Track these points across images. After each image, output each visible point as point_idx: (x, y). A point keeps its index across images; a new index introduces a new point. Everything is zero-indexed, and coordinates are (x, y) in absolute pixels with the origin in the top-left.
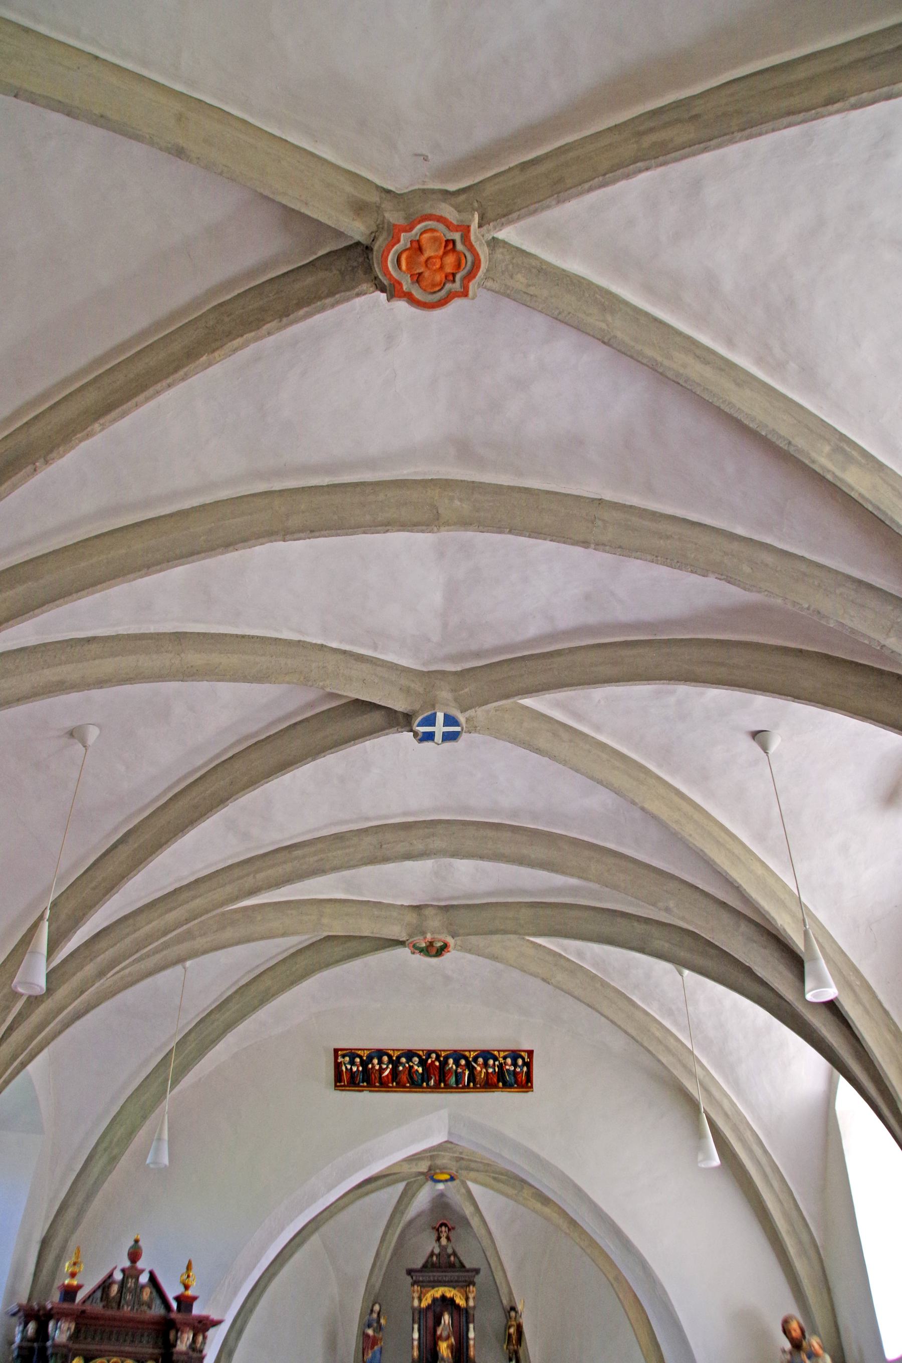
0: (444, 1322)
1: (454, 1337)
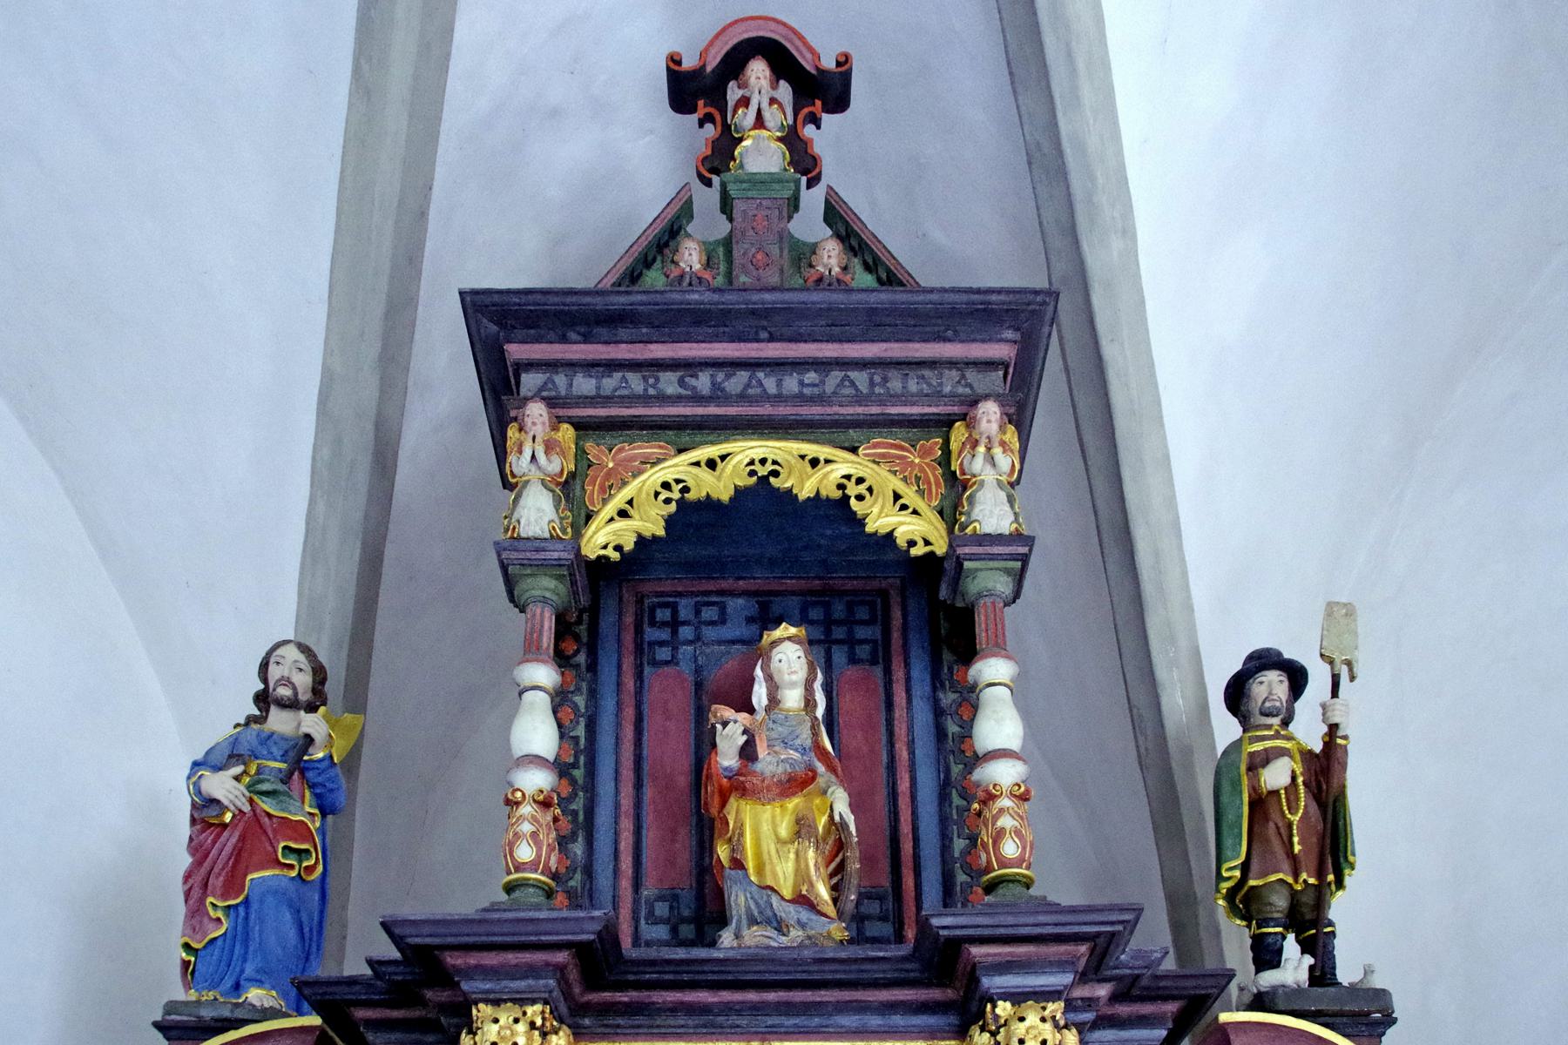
0: (774, 701)
1: (847, 782)
